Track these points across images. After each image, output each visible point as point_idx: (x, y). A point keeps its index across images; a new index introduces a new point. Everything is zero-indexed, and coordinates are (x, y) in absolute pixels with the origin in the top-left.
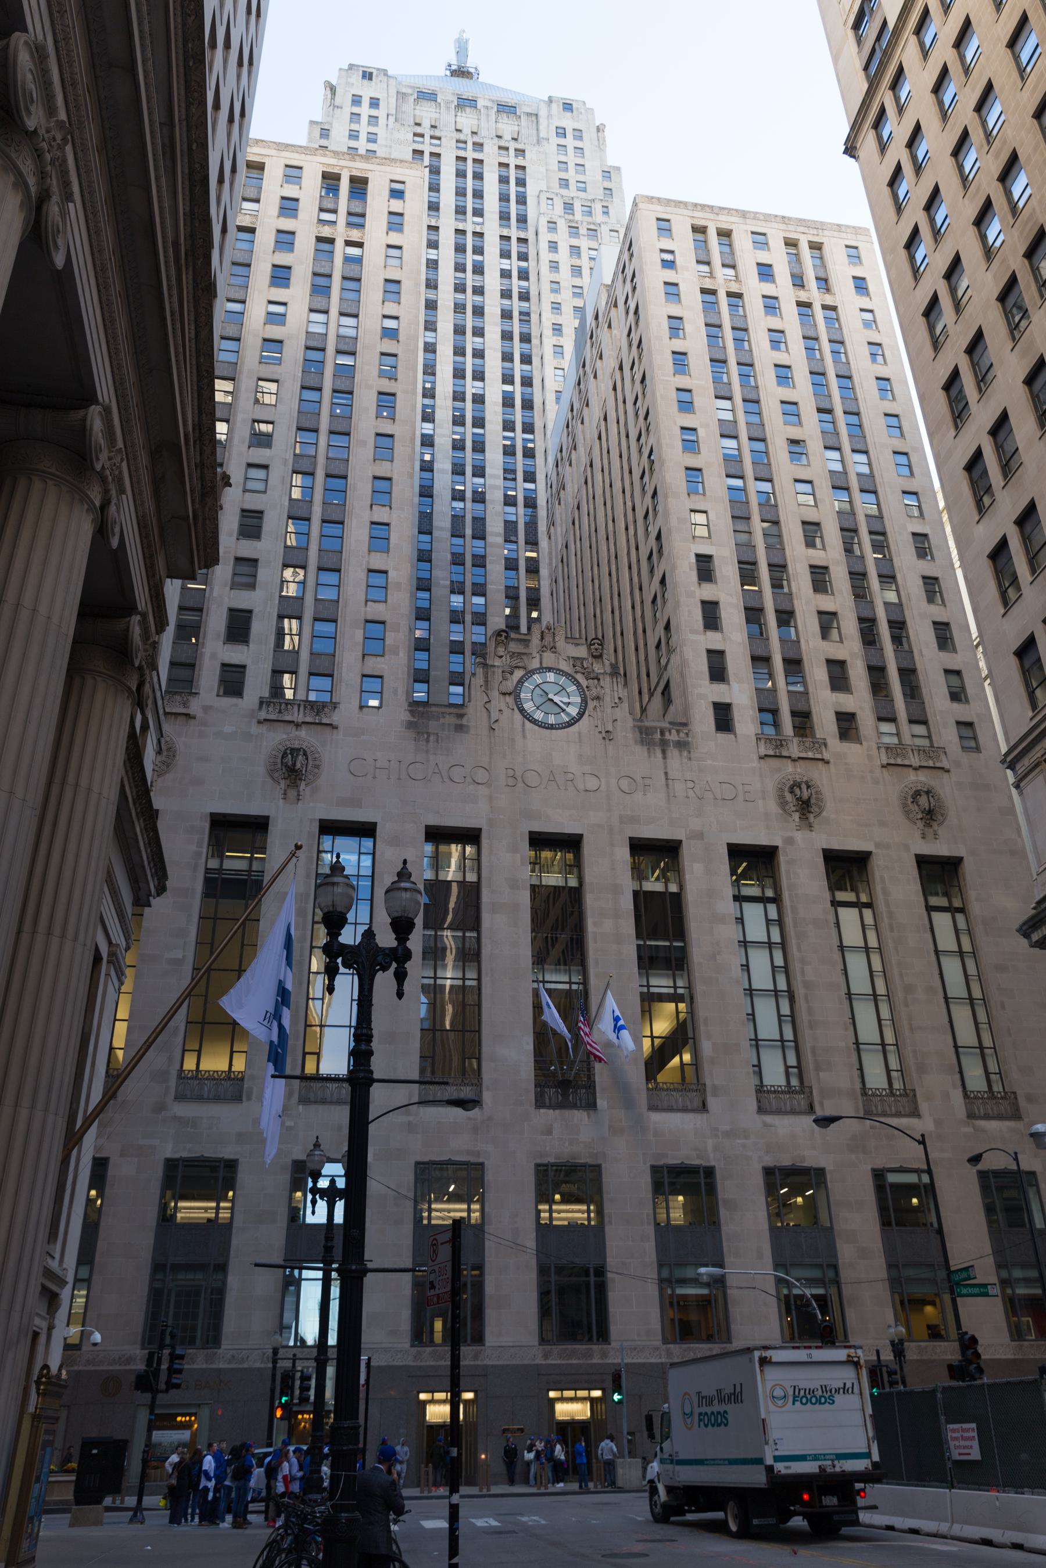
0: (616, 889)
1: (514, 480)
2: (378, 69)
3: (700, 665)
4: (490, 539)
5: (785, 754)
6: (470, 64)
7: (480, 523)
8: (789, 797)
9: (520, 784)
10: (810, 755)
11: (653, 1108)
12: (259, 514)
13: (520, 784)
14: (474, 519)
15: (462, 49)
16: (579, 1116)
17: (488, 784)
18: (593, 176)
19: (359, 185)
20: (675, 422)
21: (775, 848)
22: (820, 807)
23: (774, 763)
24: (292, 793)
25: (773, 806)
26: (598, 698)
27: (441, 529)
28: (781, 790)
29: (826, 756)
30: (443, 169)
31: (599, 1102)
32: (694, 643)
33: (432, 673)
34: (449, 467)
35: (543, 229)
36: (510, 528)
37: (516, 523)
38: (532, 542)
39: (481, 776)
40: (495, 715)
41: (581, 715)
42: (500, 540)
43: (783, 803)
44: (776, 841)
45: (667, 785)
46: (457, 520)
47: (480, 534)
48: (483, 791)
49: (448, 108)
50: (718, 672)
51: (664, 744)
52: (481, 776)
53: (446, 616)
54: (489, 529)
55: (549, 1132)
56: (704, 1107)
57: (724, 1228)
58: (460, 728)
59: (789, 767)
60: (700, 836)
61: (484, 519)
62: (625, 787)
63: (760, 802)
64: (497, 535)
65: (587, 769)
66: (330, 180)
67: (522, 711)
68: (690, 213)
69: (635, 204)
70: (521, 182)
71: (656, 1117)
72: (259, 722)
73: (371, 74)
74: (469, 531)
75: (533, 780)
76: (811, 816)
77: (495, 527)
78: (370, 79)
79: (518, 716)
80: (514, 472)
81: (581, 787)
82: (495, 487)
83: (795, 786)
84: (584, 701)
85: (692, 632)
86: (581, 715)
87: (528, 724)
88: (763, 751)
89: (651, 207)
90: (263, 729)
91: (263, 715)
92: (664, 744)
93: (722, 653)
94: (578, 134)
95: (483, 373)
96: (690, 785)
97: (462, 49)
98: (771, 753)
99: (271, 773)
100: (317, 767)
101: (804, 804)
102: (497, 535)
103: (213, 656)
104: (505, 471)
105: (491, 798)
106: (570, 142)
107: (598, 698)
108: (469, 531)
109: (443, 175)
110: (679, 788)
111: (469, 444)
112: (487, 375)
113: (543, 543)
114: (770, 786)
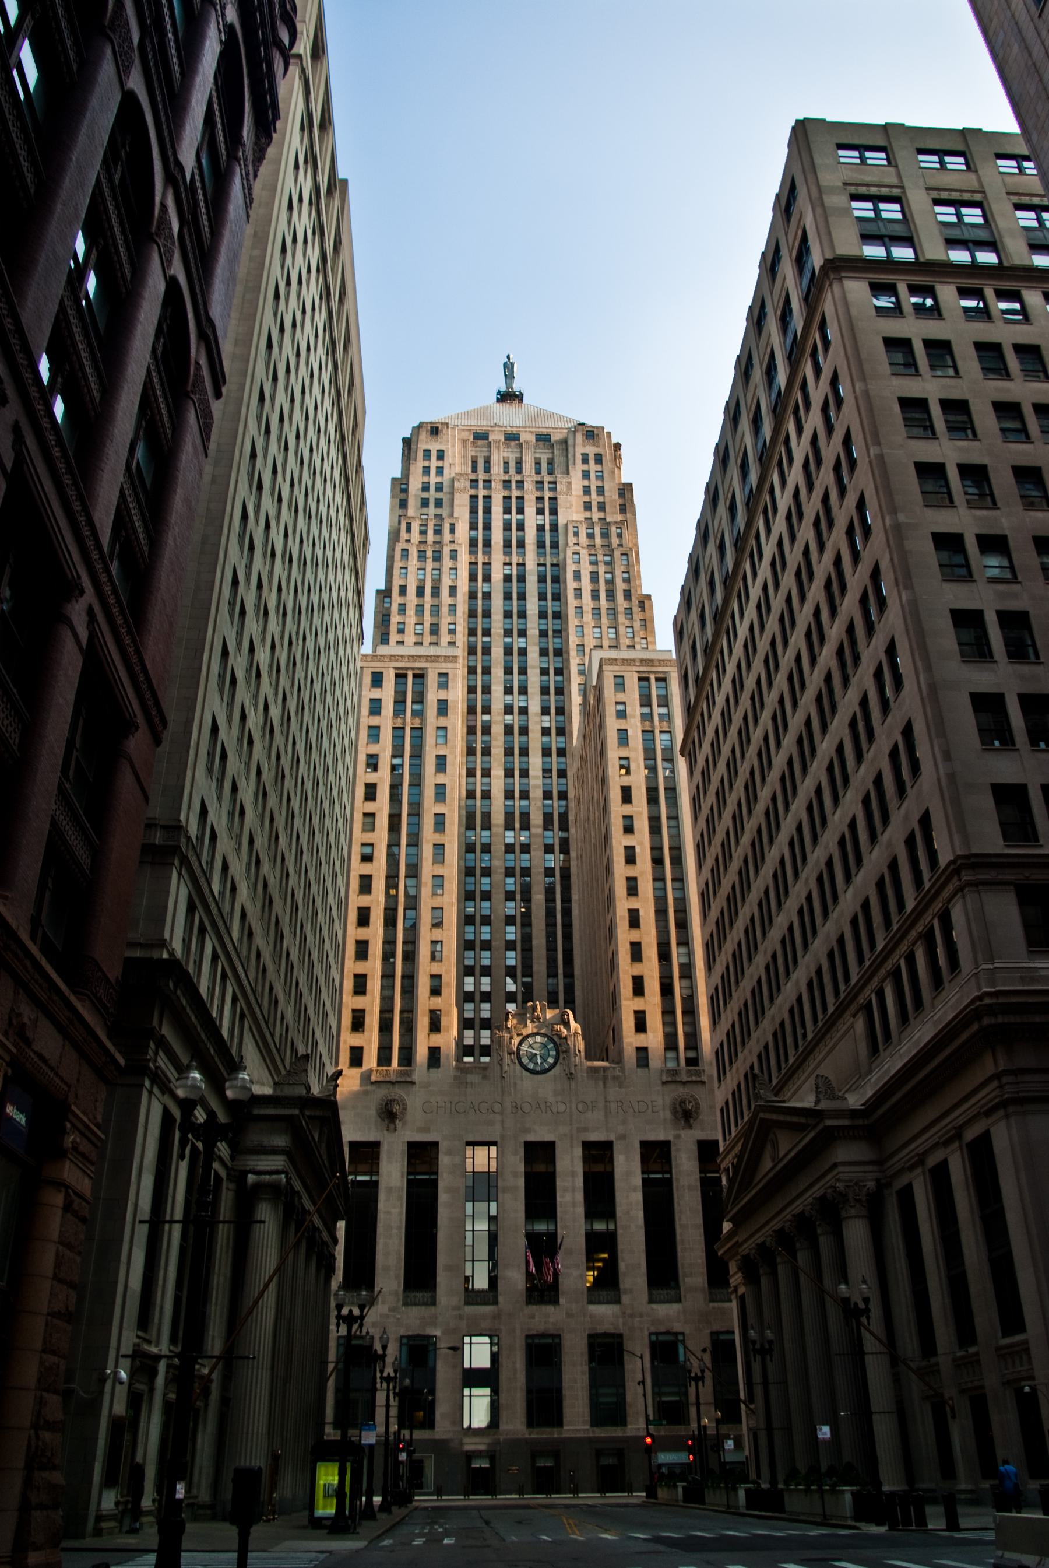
0: (573, 1174)
1: (551, 777)
2: (442, 423)
3: (628, 1023)
4: (533, 830)
5: (678, 1079)
6: (517, 387)
7: (525, 816)
8: (678, 1108)
9: (520, 1111)
10: (694, 1078)
11: (590, 1302)
12: (370, 877)
13: (520, 1111)
14: (521, 814)
15: (509, 370)
16: (550, 1309)
17: (501, 1113)
18: (612, 494)
19: (420, 676)
20: (620, 843)
21: (669, 1142)
22: (697, 1113)
23: (672, 1087)
24: (392, 1126)
25: (668, 1115)
26: (565, 1052)
27: (497, 826)
28: (674, 1104)
29: (704, 1078)
30: (493, 509)
31: (561, 1300)
32: (628, 1005)
33: (493, 944)
34: (502, 773)
35: (569, 561)
36: (548, 818)
37: (552, 814)
38: (564, 826)
39: (497, 1107)
40: (506, 1068)
41: (555, 1063)
42: (540, 830)
43: (674, 1112)
44: (670, 1138)
45: (606, 1106)
46: (509, 816)
47: (526, 826)
48: (498, 1117)
49: (497, 447)
50: (641, 1026)
51: (605, 1079)
52: (497, 1107)
53: (502, 896)
54: (532, 822)
55: (533, 1317)
56: (618, 1301)
57: (626, 1367)
58: (485, 1077)
59: (681, 1089)
60: (623, 1137)
61: (528, 814)
62: (580, 1109)
63: (661, 1112)
64: (538, 826)
65: (559, 1098)
66: (400, 676)
67: (521, 1063)
68: (638, 669)
69: (600, 666)
70: (554, 512)
71: (592, 1308)
72: (372, 1083)
73: (437, 428)
74: (517, 826)
75: (527, 1107)
76: (692, 1121)
77: (536, 818)
78: (437, 433)
79: (518, 1067)
80: (550, 771)
81: (555, 1110)
82: (536, 787)
83: (682, 1102)
84: (558, 1053)
85: (627, 999)
86: (555, 1063)
87: (524, 1072)
88: (664, 1079)
89: (611, 668)
90: (373, 1087)
91: (373, 1078)
92: (605, 1079)
93: (644, 1012)
94: (599, 459)
95: (526, 688)
96: (620, 1104)
97: (509, 370)
98: (670, 1079)
99: (379, 1115)
100: (405, 1109)
101: (685, 1114)
102: (538, 826)
103: (345, 1042)
104: (544, 771)
105: (502, 1122)
106: (593, 467)
107: (565, 1052)
108: (517, 826)
109: (493, 516)
110: (613, 1106)
111: (516, 751)
112: (529, 690)
113: (572, 830)
114: (668, 1100)
